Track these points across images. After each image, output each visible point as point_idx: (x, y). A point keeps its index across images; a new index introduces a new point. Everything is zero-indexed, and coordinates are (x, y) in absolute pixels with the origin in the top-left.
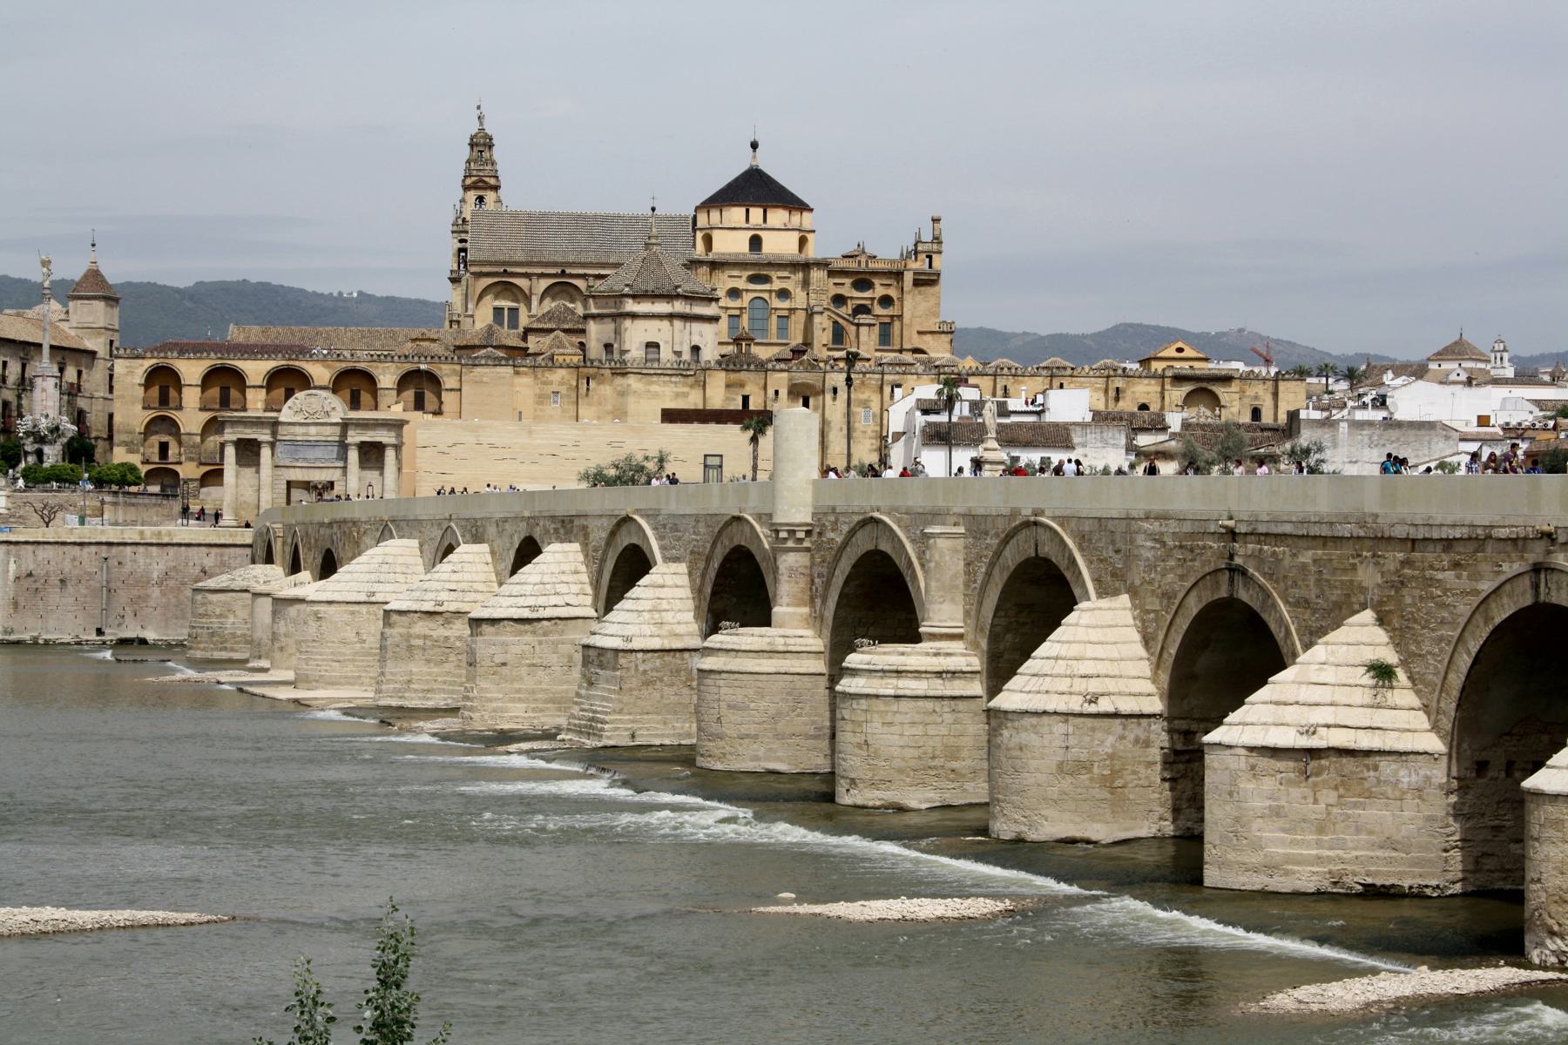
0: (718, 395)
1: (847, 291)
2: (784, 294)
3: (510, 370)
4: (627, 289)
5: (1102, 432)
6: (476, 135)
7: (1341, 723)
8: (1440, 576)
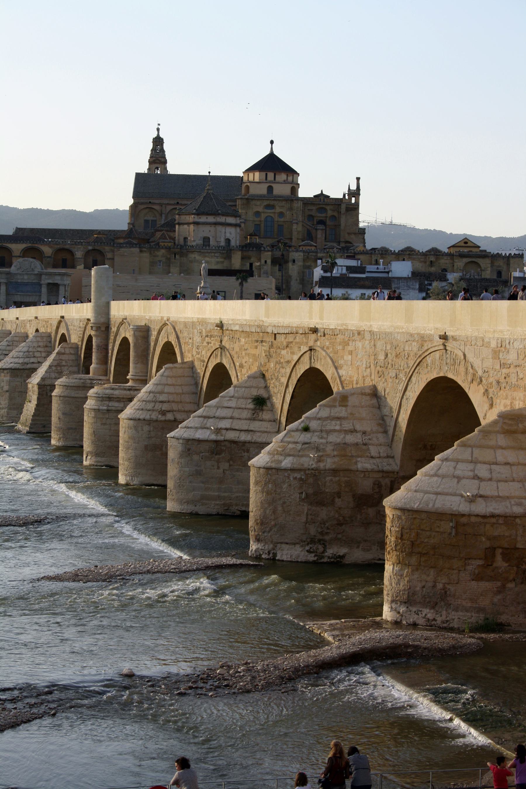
0: (236, 262)
1: (313, 213)
2: (281, 214)
3: (137, 250)
4: (194, 211)
5: (407, 282)
6: (156, 138)
7: (234, 428)
8: (284, 352)
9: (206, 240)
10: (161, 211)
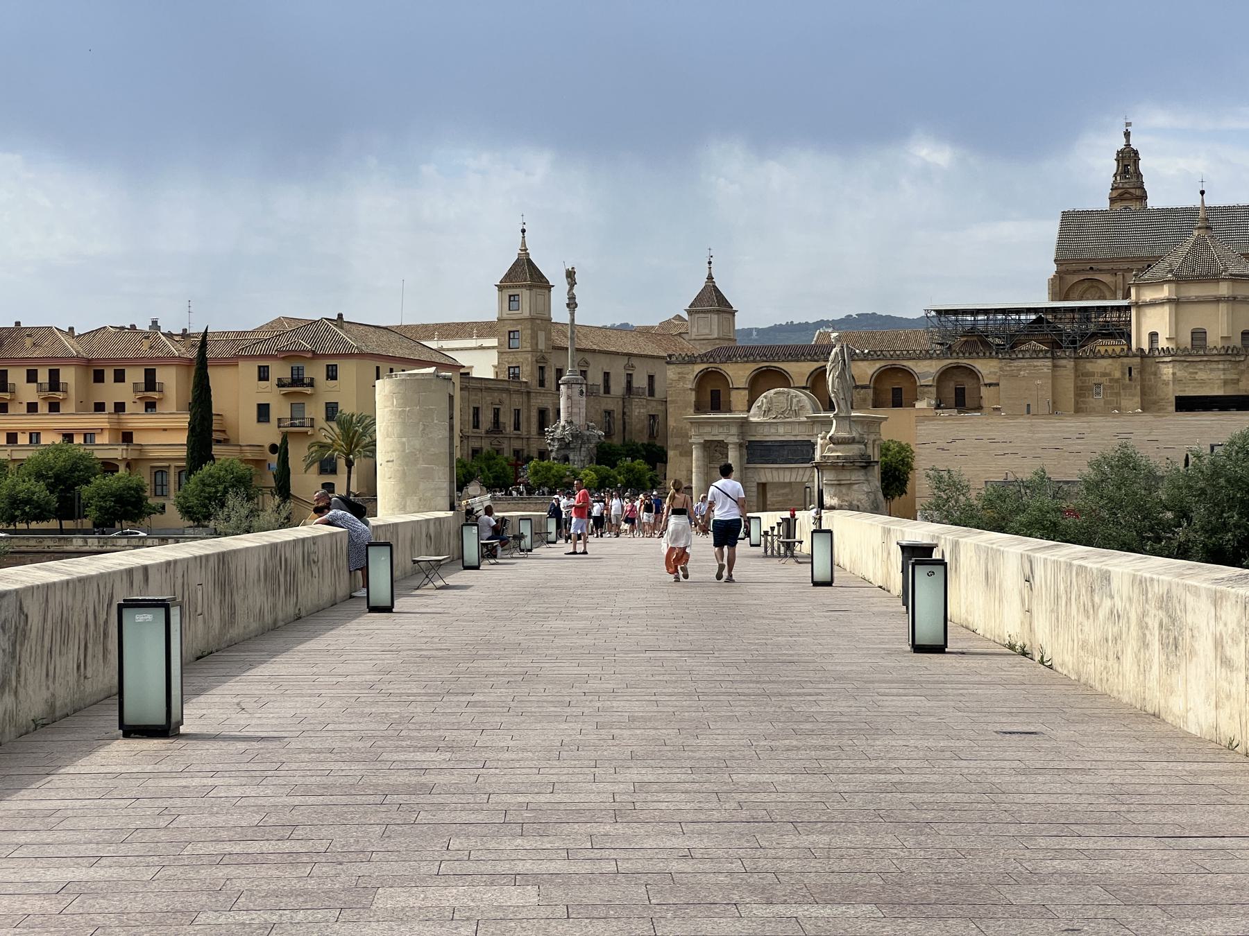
3: (1049, 363)
6: (1122, 151)
9: (1199, 336)
10: (1116, 287)
